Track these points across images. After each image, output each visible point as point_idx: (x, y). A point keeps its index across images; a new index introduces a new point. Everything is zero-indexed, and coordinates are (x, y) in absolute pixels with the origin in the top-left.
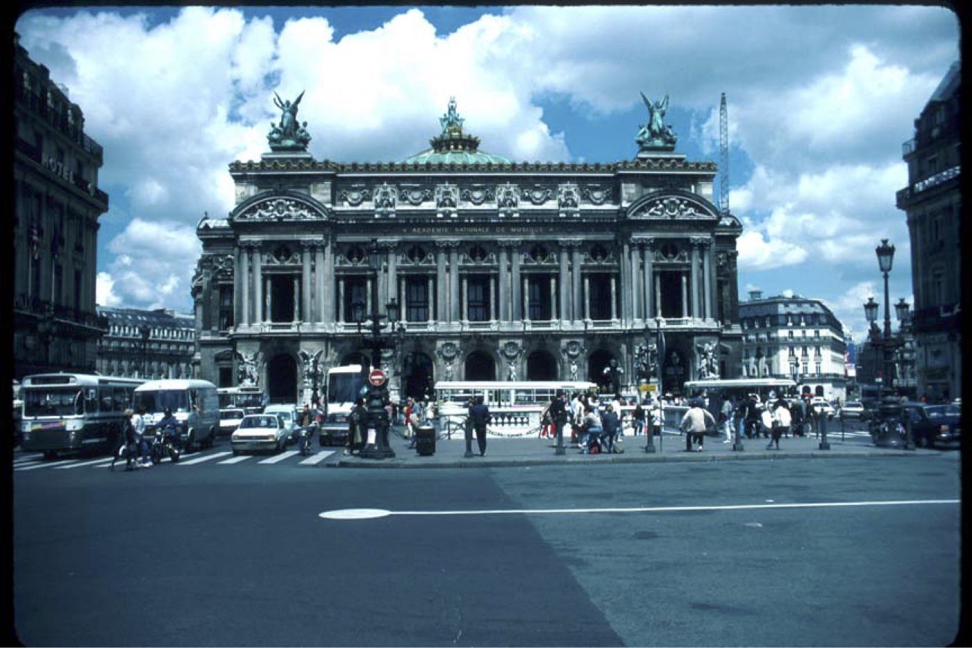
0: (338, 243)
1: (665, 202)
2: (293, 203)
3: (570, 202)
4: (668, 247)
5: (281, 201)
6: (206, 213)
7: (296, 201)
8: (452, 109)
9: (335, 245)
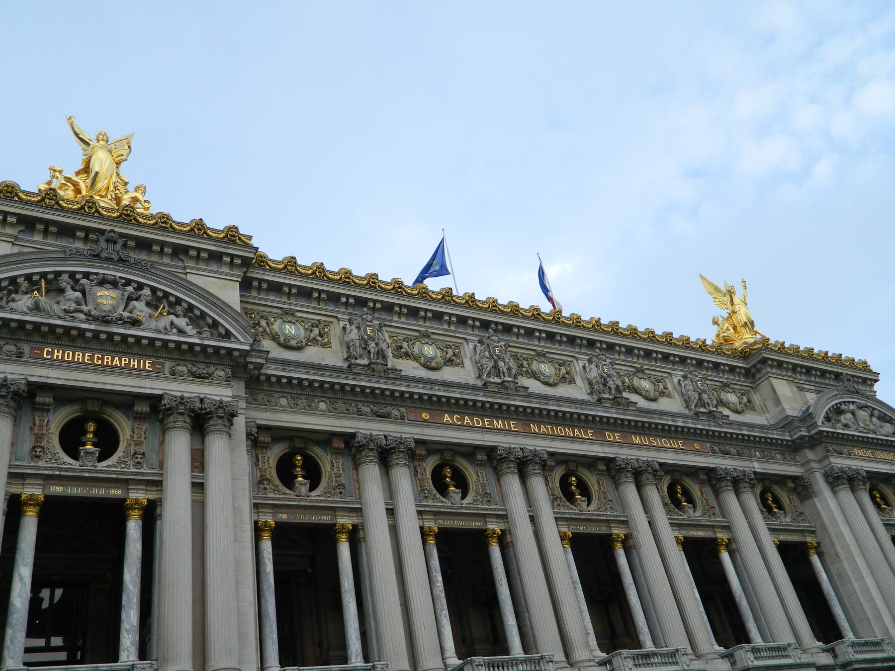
2: (146, 292)
7: (154, 290)
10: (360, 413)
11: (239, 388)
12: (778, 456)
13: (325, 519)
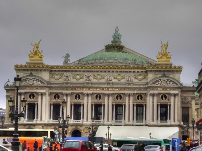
0: (51, 93)
1: (162, 80)
2: (35, 79)
3: (130, 79)
4: (164, 96)
5: (31, 79)
6: (8, 80)
7: (36, 79)
8: (117, 31)
9: (50, 94)
10: (64, 90)
11: (47, 89)
12: (142, 90)
13: (59, 103)
